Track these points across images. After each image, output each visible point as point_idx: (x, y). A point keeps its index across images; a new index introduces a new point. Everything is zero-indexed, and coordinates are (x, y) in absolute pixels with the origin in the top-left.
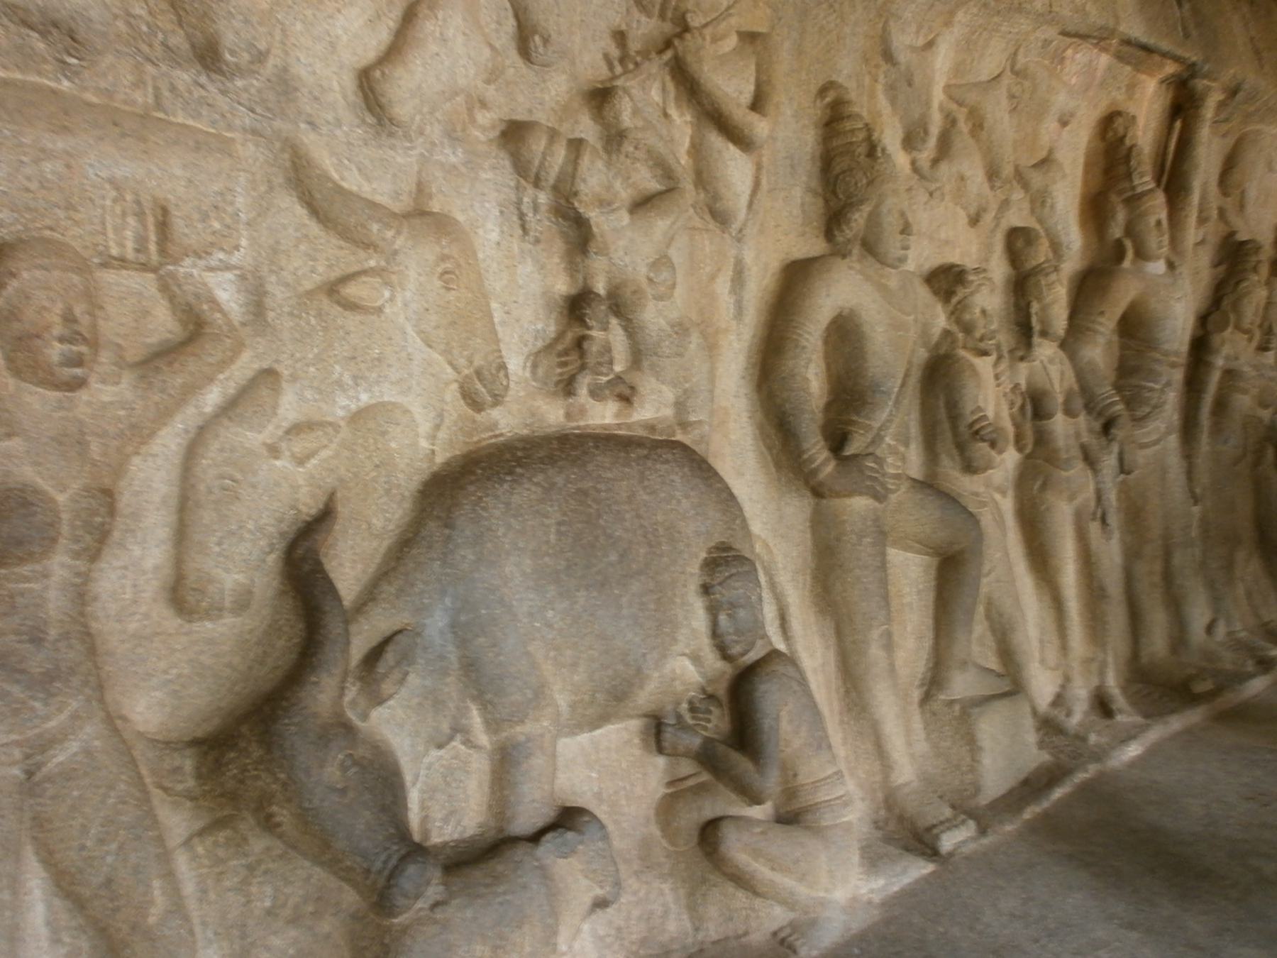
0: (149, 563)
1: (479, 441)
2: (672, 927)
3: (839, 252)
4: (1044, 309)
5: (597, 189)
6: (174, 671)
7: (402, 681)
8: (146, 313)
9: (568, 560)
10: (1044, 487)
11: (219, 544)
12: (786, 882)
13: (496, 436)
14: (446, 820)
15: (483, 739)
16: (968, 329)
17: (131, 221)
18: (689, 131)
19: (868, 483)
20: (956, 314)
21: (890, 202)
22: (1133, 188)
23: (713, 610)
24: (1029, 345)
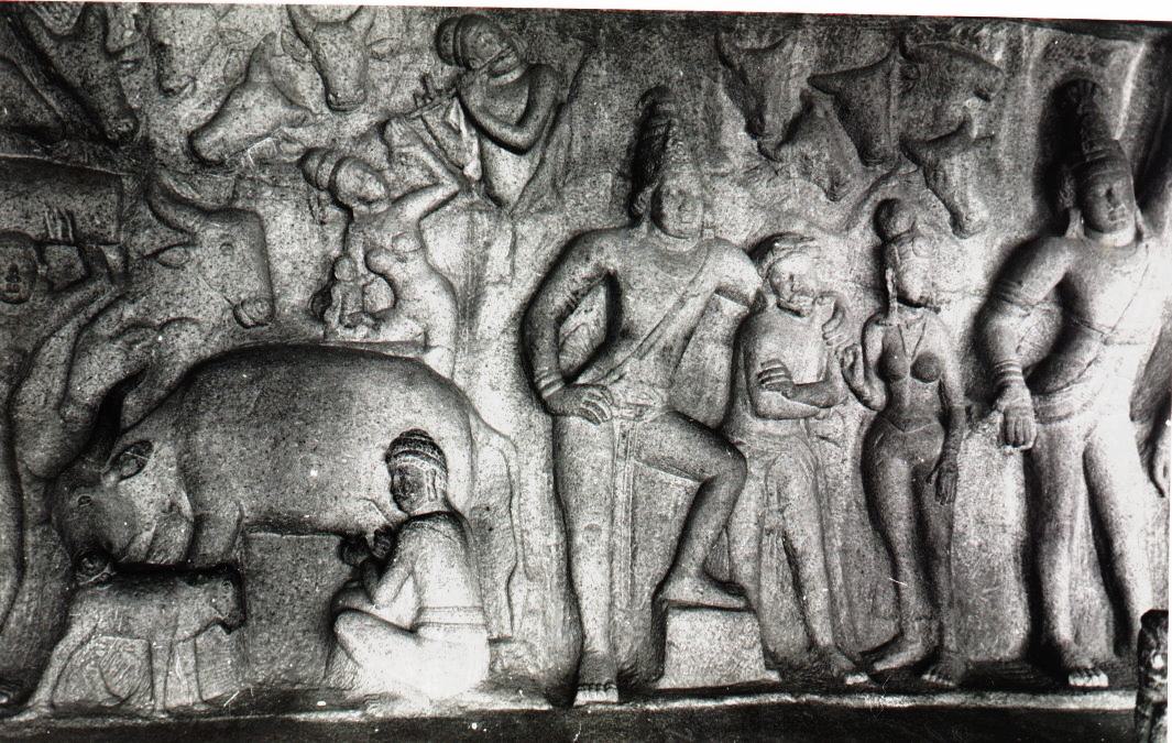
3: (635, 220)
4: (899, 276)
5: (353, 189)
8: (72, 266)
10: (881, 443)
16: (776, 291)
17: (59, 222)
18: (475, 141)
20: (769, 275)
21: (671, 183)
22: (1083, 157)
23: (392, 473)
24: (885, 310)
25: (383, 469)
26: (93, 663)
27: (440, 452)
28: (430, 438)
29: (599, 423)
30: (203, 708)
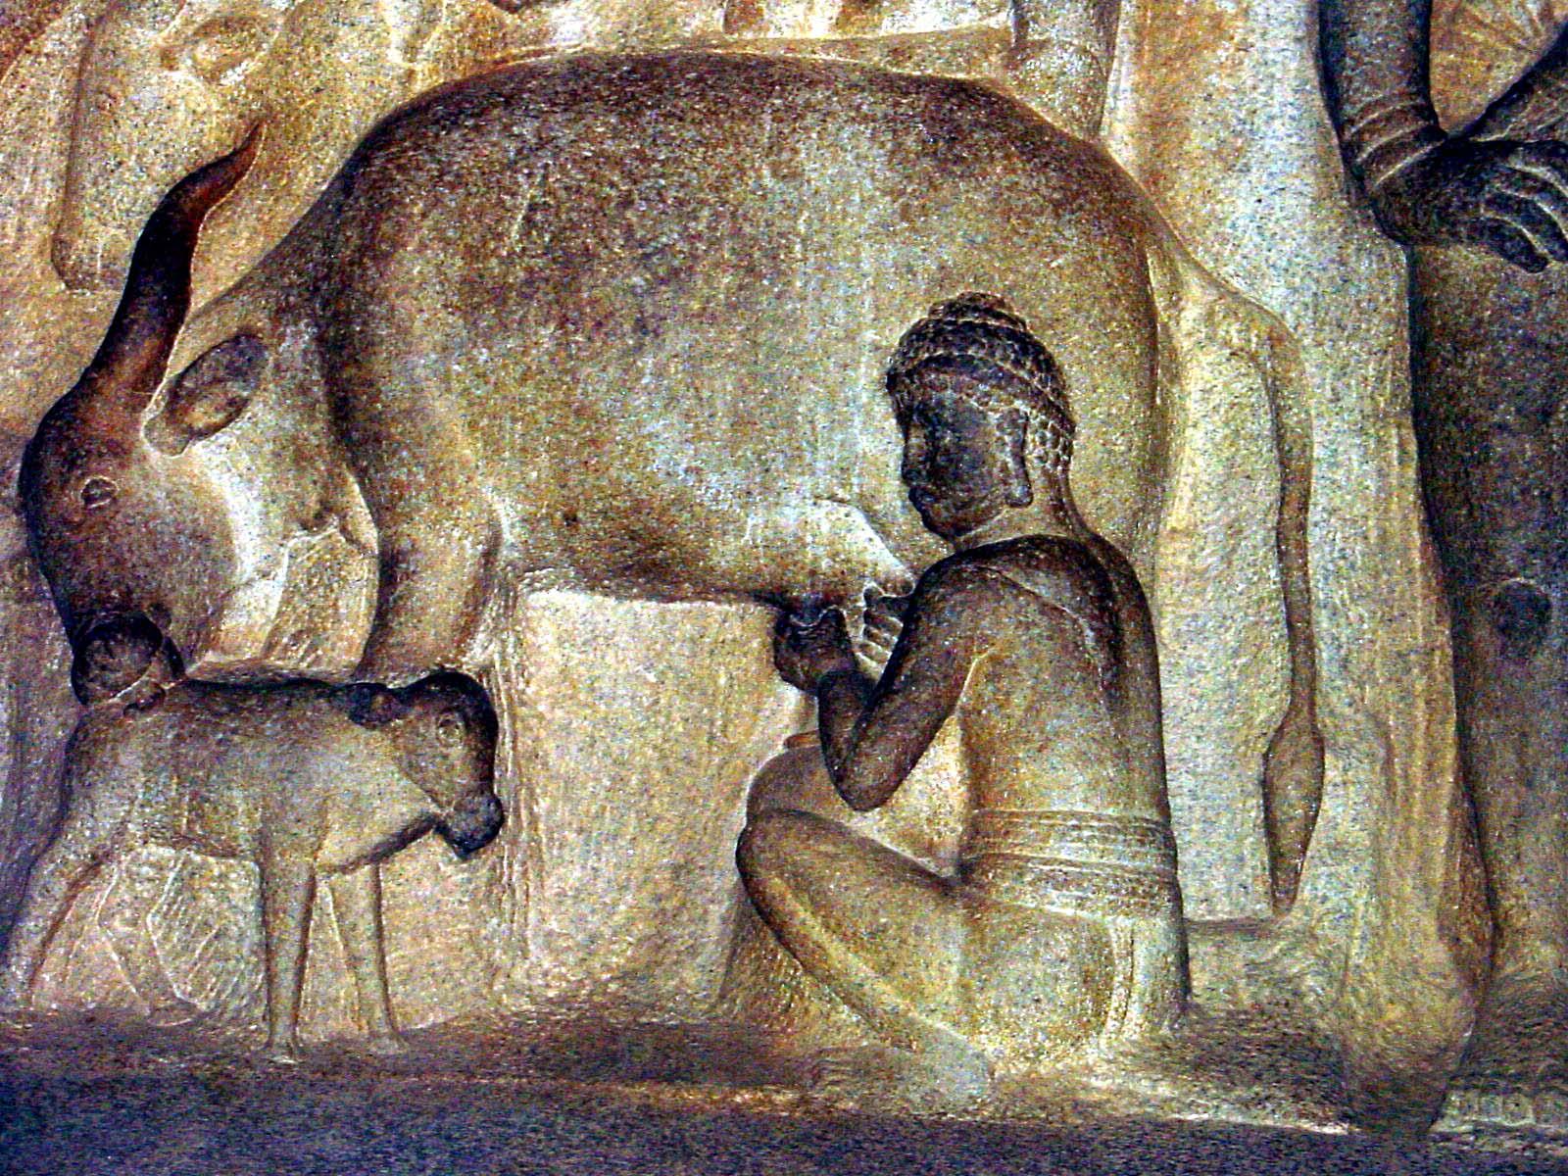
0: (42, 203)
1: (504, 60)
2: (691, 976)
6: (40, 348)
7: (236, 408)
9: (530, 270)
11: (95, 184)
12: (858, 967)
13: (538, 54)
14: (296, 638)
15: (370, 534)
19: (1487, 214)
23: (904, 419)
25: (883, 411)
26: (128, 914)
27: (1047, 365)
28: (1015, 321)
29: (1539, 263)
30: (393, 1048)
